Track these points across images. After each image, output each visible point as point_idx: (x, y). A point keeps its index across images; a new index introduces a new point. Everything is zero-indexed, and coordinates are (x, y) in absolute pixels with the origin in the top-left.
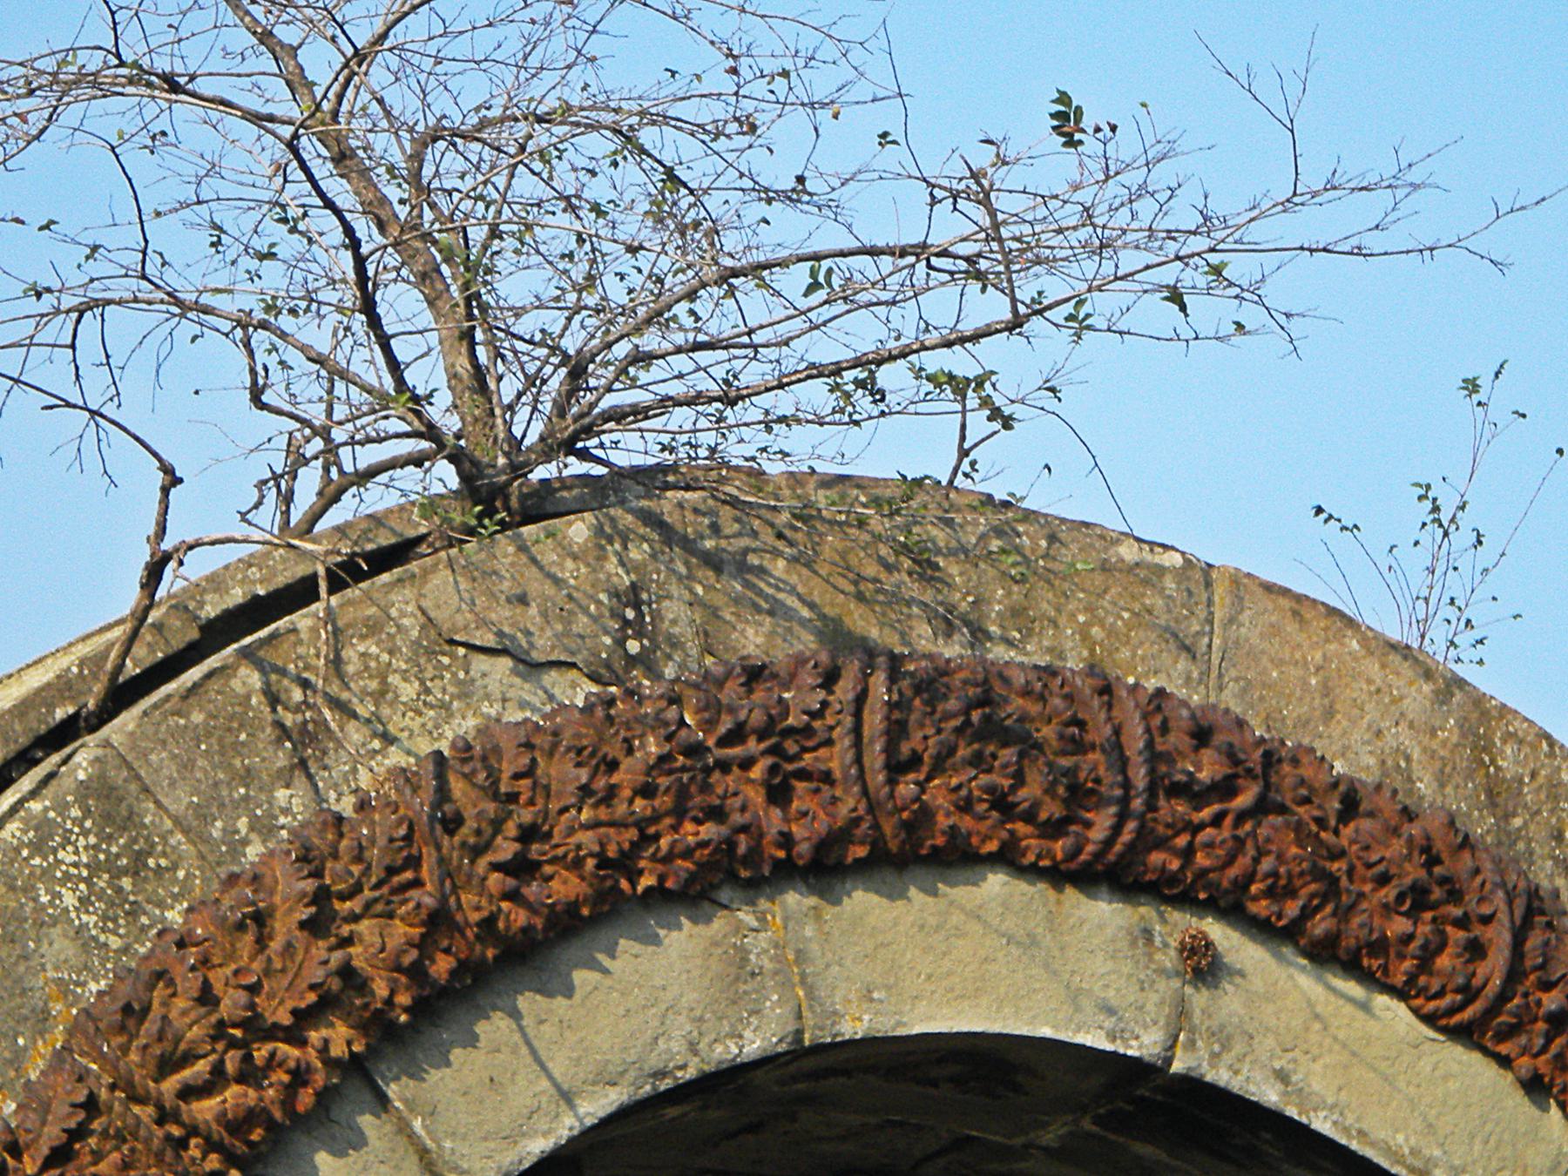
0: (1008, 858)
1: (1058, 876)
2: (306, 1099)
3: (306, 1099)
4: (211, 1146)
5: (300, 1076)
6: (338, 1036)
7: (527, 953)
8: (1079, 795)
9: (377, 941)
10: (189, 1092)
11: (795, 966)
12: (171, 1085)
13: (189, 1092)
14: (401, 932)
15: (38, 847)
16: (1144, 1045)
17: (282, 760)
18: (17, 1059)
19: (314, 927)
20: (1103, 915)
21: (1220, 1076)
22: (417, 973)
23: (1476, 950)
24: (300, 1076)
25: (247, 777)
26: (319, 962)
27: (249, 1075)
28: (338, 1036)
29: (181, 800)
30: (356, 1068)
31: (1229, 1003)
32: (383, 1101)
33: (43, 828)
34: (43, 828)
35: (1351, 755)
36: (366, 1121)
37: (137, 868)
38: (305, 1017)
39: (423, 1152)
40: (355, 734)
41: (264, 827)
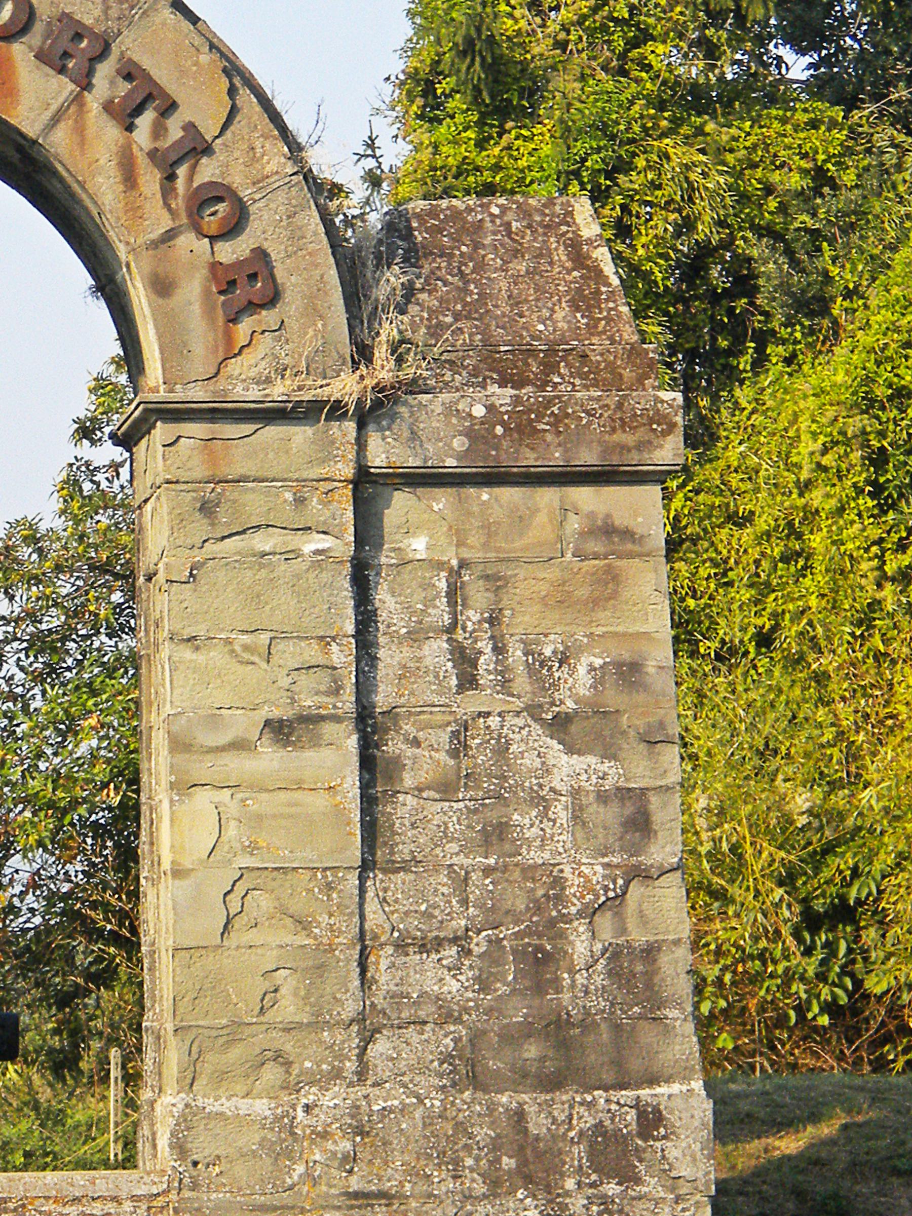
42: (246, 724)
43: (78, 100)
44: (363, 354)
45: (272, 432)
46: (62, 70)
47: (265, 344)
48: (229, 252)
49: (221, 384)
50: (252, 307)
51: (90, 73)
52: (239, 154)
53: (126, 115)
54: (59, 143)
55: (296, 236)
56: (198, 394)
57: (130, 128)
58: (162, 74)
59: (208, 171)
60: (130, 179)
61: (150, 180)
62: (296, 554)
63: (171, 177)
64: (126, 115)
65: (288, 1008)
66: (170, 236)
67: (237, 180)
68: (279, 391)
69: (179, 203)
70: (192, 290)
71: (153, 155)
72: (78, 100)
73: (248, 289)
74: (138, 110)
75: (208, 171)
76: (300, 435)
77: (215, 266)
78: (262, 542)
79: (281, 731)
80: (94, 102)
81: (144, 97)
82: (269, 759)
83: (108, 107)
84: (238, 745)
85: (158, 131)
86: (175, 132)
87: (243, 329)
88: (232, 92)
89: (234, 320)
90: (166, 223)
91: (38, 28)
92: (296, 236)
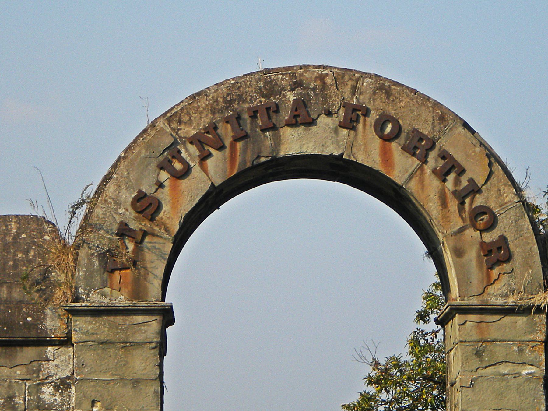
43: (421, 168)
45: (508, 319)
46: (414, 155)
47: (505, 279)
48: (488, 237)
49: (485, 297)
50: (499, 262)
51: (426, 156)
52: (493, 193)
53: (442, 175)
54: (413, 187)
55: (519, 230)
56: (474, 302)
57: (444, 181)
58: (459, 157)
59: (479, 200)
60: (444, 204)
61: (453, 205)
62: (517, 375)
63: (462, 203)
64: (442, 175)
66: (462, 230)
67: (492, 204)
68: (511, 301)
69: (466, 215)
70: (472, 254)
71: (454, 193)
72: (421, 168)
73: (497, 254)
74: (448, 173)
75: (479, 200)
76: (521, 320)
77: (482, 244)
78: (504, 369)
80: (428, 169)
81: (450, 167)
83: (434, 171)
85: (457, 182)
86: (464, 183)
87: (495, 272)
88: (490, 165)
89: (491, 268)
90: (460, 224)
91: (403, 135)
92: (519, 230)
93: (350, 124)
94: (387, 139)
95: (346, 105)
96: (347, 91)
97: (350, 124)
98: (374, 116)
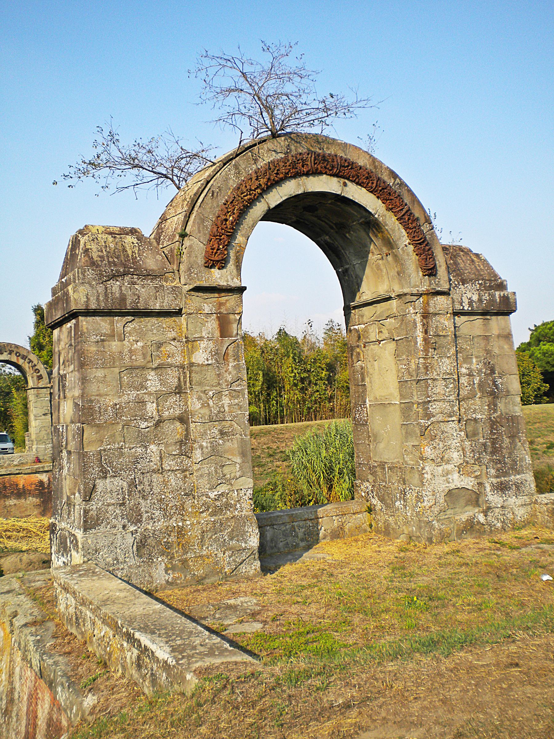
0: (326, 173)
1: (331, 175)
2: (256, 197)
3: (256, 197)
4: (246, 202)
5: (255, 195)
6: (259, 191)
7: (278, 183)
8: (333, 167)
9: (263, 181)
10: (244, 196)
11: (304, 184)
12: (242, 195)
13: (244, 196)
14: (265, 180)
15: (229, 171)
16: (339, 193)
17: (253, 162)
18: (227, 193)
19: (257, 179)
20: (335, 179)
21: (346, 196)
22: (267, 184)
23: (373, 183)
24: (255, 195)
25: (250, 164)
26: (257, 183)
27: (250, 195)
28: (259, 191)
29: (243, 166)
30: (261, 194)
31: (347, 189)
32: (263, 197)
33: (230, 169)
34: (230, 169)
35: (361, 163)
36: (262, 199)
37: (239, 174)
38: (256, 189)
39: (267, 203)
40: (260, 160)
41: (252, 169)
42: (41, 414)
44: (50, 383)
48: (38, 374)
53: (29, 363)
54: (23, 365)
56: (36, 387)
58: (32, 359)
59: (36, 367)
60: (29, 368)
61: (31, 368)
64: (29, 363)
65: (45, 438)
68: (43, 386)
70: (35, 378)
73: (40, 377)
75: (36, 367)
79: (44, 415)
81: (30, 361)
82: (43, 417)
84: (41, 416)
86: (33, 364)
93: (10, 354)
94: (18, 356)
95: (9, 350)
96: (9, 347)
97: (10, 354)
98: (15, 352)
